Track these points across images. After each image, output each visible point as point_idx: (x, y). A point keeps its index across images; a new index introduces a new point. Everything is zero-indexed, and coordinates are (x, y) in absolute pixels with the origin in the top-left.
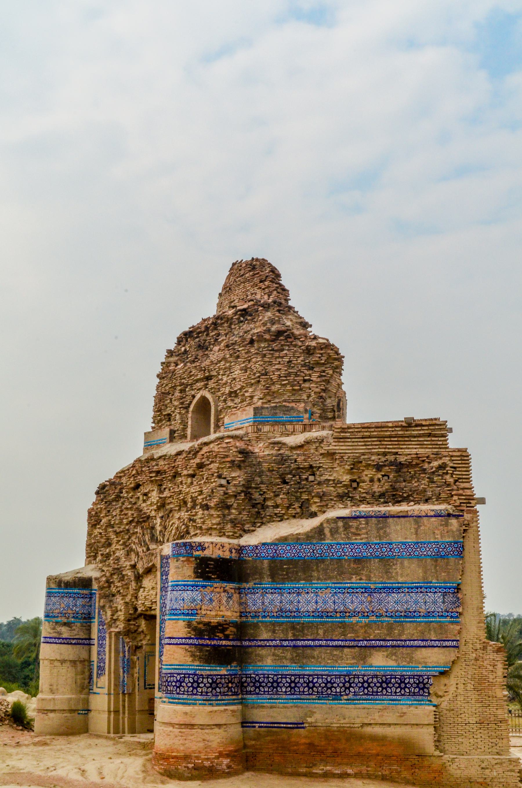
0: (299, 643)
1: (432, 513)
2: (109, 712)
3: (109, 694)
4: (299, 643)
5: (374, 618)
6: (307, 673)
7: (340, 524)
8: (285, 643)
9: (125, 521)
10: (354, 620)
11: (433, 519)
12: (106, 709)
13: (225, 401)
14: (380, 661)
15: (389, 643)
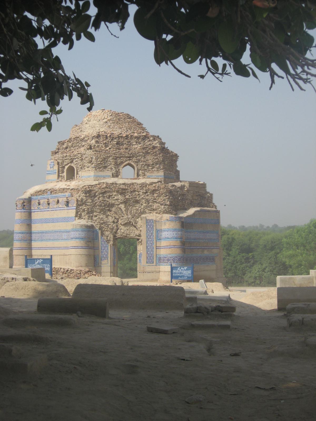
0: (191, 248)
1: (214, 211)
2: (111, 272)
3: (111, 266)
4: (191, 248)
5: (204, 240)
6: (193, 256)
7: (198, 213)
8: (189, 248)
9: (103, 205)
10: (201, 241)
11: (214, 213)
12: (110, 271)
13: (144, 167)
14: (206, 252)
15: (208, 247)
